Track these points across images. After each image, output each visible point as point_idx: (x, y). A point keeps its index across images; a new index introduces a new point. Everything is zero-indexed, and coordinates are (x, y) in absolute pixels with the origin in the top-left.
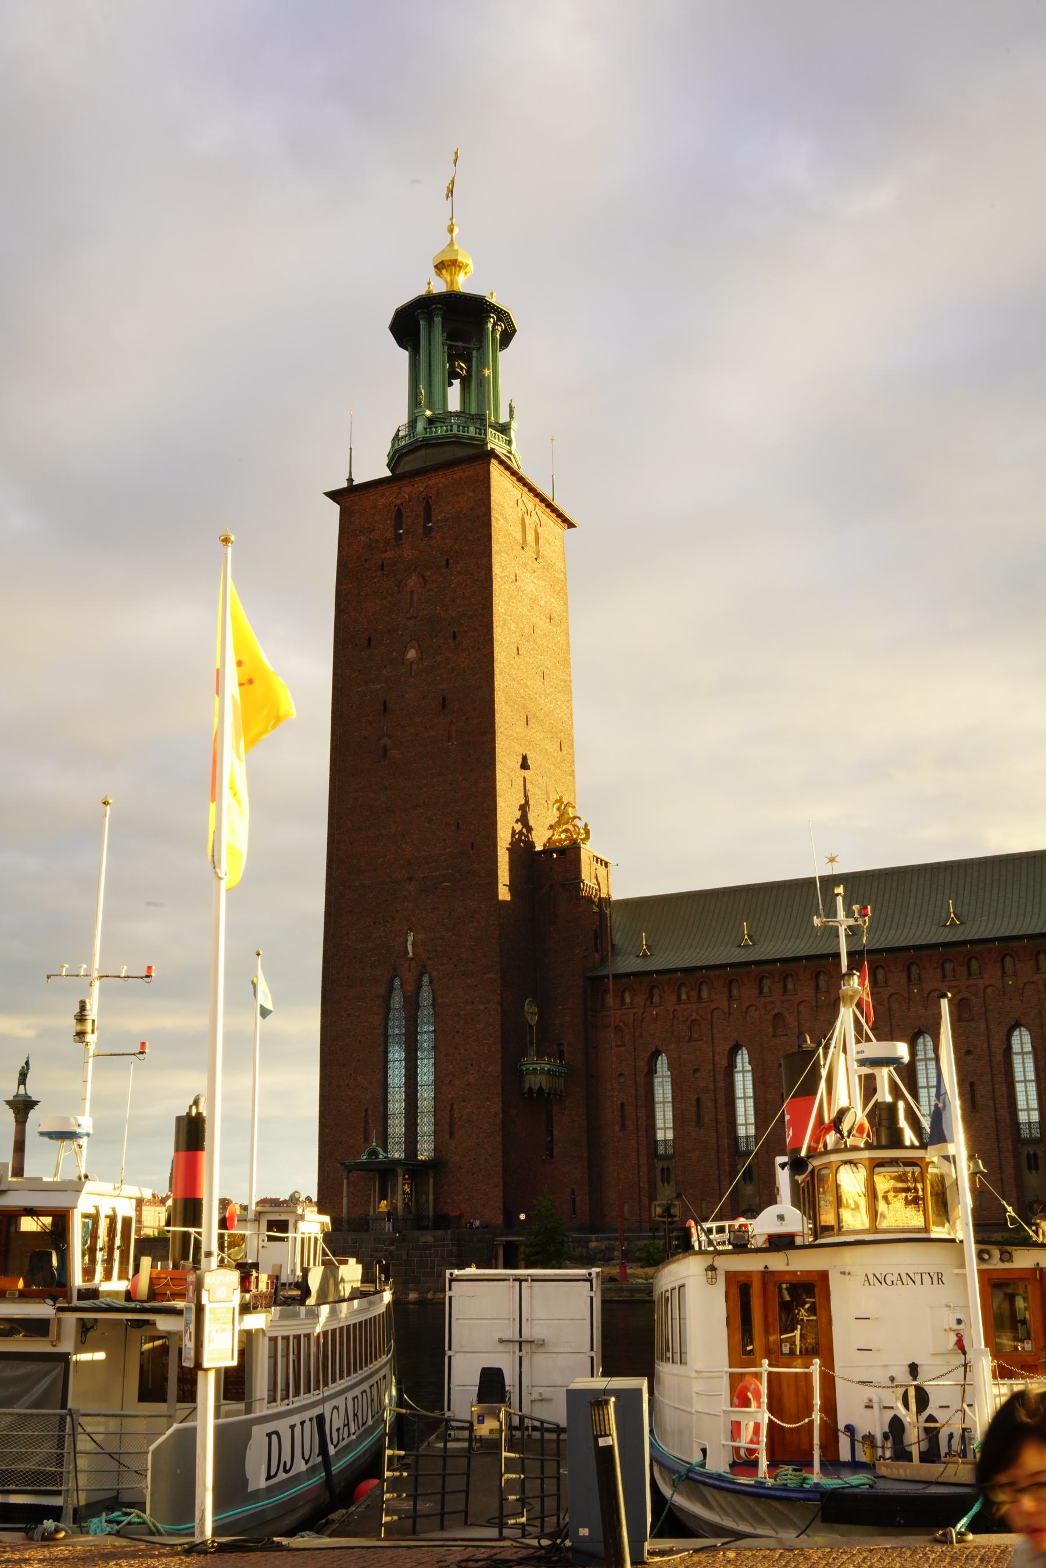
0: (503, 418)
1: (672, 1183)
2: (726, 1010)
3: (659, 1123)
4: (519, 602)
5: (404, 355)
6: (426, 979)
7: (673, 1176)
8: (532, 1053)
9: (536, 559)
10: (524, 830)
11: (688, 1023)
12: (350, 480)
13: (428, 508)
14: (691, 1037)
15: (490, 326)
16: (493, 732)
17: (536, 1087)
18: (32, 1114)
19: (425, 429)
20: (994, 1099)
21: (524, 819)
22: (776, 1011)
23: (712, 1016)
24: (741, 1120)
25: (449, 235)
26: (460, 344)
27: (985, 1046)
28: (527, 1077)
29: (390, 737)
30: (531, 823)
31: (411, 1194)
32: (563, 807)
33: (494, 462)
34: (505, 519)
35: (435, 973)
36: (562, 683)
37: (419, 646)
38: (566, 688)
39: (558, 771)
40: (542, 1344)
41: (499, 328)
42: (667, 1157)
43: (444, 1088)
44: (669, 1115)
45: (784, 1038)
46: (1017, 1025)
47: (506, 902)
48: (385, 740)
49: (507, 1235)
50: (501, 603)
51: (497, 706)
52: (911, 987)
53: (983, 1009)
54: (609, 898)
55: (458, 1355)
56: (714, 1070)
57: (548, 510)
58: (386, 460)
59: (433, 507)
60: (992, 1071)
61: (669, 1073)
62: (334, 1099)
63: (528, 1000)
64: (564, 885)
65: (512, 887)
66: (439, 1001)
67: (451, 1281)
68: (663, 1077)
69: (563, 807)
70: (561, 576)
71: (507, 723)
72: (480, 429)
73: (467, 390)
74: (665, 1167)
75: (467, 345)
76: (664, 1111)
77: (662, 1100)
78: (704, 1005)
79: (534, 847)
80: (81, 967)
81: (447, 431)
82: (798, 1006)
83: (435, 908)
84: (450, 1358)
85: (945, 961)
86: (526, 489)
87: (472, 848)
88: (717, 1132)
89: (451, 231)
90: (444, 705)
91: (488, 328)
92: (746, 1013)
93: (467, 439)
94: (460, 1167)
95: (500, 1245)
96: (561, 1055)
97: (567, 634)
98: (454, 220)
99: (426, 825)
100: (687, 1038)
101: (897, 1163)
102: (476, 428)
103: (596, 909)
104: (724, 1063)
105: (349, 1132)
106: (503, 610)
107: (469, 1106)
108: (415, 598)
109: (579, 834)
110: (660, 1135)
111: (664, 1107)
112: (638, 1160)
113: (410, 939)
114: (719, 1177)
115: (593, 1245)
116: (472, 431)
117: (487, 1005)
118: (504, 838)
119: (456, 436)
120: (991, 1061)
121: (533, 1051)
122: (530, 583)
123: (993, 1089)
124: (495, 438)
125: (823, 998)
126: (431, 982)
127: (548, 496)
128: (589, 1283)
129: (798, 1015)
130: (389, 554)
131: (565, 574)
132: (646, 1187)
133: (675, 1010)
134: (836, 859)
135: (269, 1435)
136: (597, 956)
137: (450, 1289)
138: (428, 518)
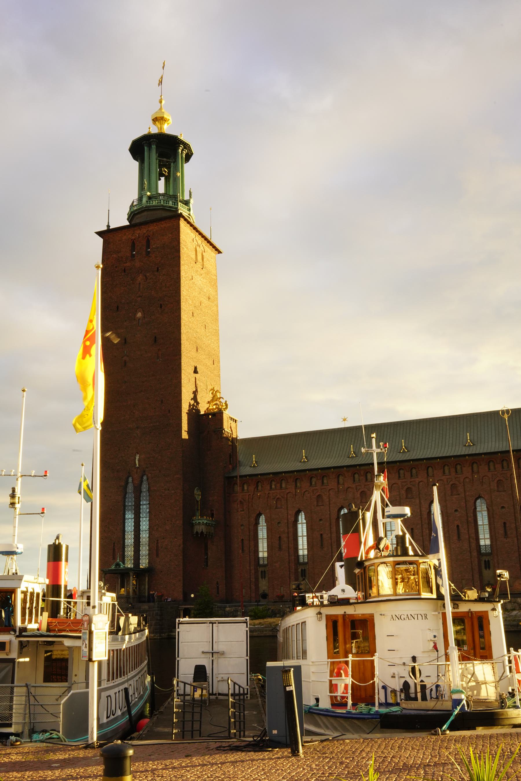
0: (186, 198)
1: (267, 578)
2: (294, 493)
3: (260, 549)
4: (194, 290)
5: (136, 164)
6: (145, 478)
7: (267, 575)
9: (202, 268)
10: (195, 404)
11: (275, 500)
12: (108, 226)
13: (148, 242)
15: (180, 151)
16: (180, 355)
17: (200, 531)
19: (147, 202)
20: (423, 536)
21: (195, 398)
22: (318, 494)
23: (287, 496)
24: (300, 547)
25: (160, 104)
26: (165, 159)
27: (419, 511)
30: (199, 400)
31: (137, 585)
32: (214, 392)
33: (182, 219)
34: (187, 248)
35: (150, 475)
36: (215, 331)
38: (216, 333)
39: (212, 375)
40: (223, 653)
41: (185, 152)
42: (264, 566)
43: (154, 532)
44: (265, 545)
45: (321, 507)
46: (479, 497)
47: (185, 439)
49: (185, 605)
50: (185, 290)
51: (182, 342)
54: (237, 438)
55: (182, 660)
56: (288, 523)
57: (208, 244)
58: (127, 217)
59: (151, 241)
61: (266, 524)
63: (196, 489)
64: (215, 431)
65: (189, 432)
66: (152, 489)
67: (179, 624)
68: (262, 526)
69: (215, 393)
70: (214, 277)
71: (187, 350)
72: (175, 203)
73: (168, 183)
74: (263, 570)
75: (168, 160)
76: (263, 543)
77: (262, 537)
78: (283, 490)
79: (200, 412)
80: (12, 471)
81: (158, 203)
82: (329, 491)
84: (178, 661)
85: (400, 469)
86: (197, 234)
87: (169, 412)
88: (289, 554)
89: (161, 102)
90: (155, 341)
91: (179, 152)
93: (167, 207)
94: (161, 572)
95: (181, 610)
96: (212, 515)
97: (217, 306)
98: (162, 97)
100: (275, 507)
101: (406, 563)
102: (173, 202)
103: (230, 443)
104: (293, 519)
106: (186, 294)
108: (141, 287)
109: (222, 406)
110: (261, 555)
111: (263, 541)
112: (250, 567)
113: (137, 457)
115: (228, 609)
116: (171, 204)
118: (185, 408)
119: (162, 206)
120: (421, 518)
121: (198, 513)
122: (199, 281)
123: (422, 532)
124: (182, 207)
126: (148, 479)
127: (208, 237)
128: (246, 624)
130: (128, 264)
131: (216, 276)
132: (254, 580)
133: (269, 493)
134: (347, 419)
135: (107, 697)
136: (230, 466)
137: (178, 628)
138: (148, 246)
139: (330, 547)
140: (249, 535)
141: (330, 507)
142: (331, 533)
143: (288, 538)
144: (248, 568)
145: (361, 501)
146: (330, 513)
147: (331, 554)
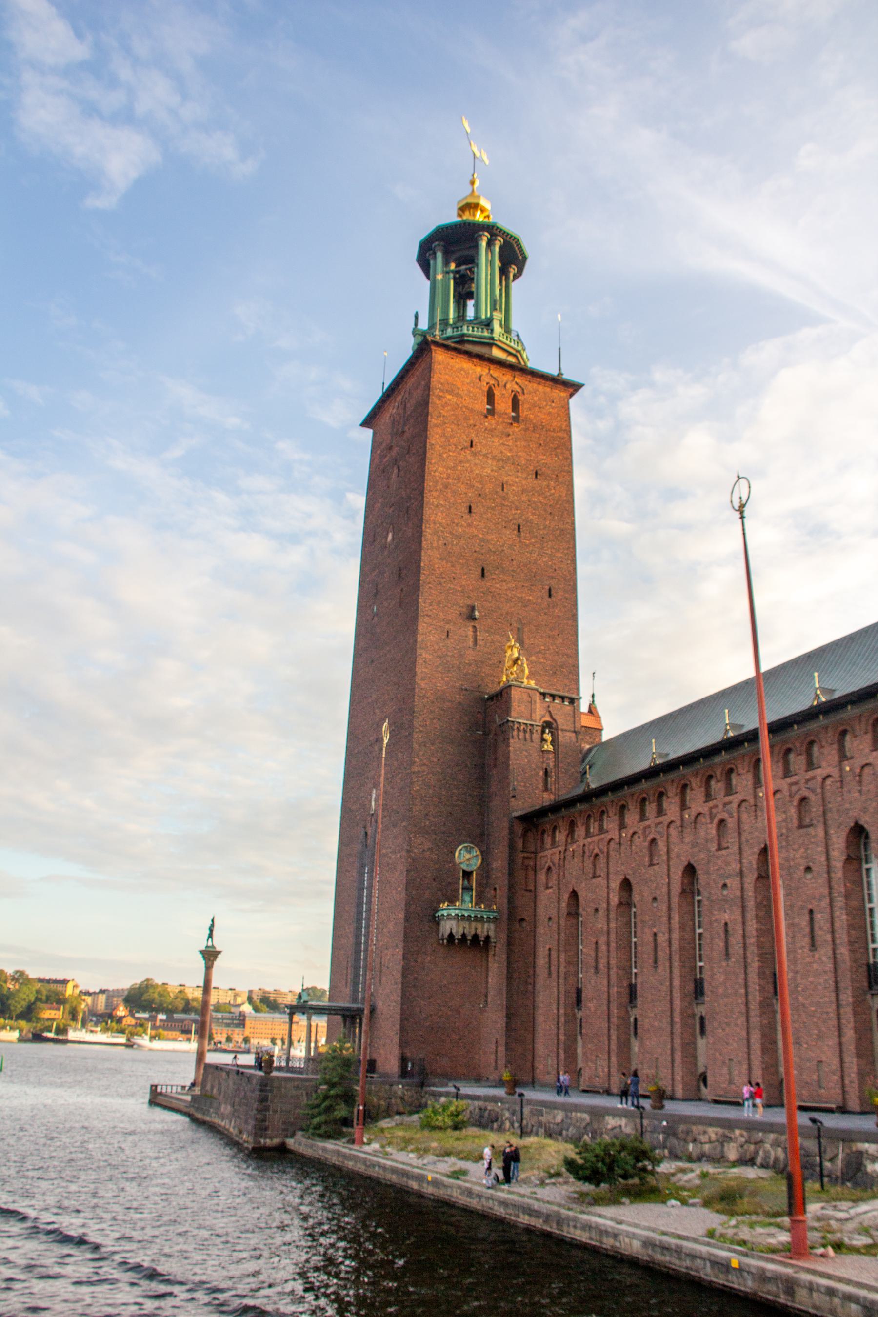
8: (467, 898)
11: (592, 858)
14: (594, 873)
18: (218, 963)
20: (833, 932)
22: (651, 836)
27: (823, 859)
28: (442, 923)
34: (457, 395)
50: (440, 469)
52: (758, 790)
53: (821, 809)
60: (830, 893)
71: (443, 578)
78: (603, 836)
82: (668, 826)
92: (631, 841)
100: (591, 875)
112: (558, 1009)
114: (609, 1030)
129: (668, 838)
133: (584, 845)
139: (667, 964)
140: (558, 940)
141: (668, 866)
142: (670, 930)
143: (608, 944)
144: (555, 1011)
145: (719, 845)
146: (669, 884)
147: (668, 984)
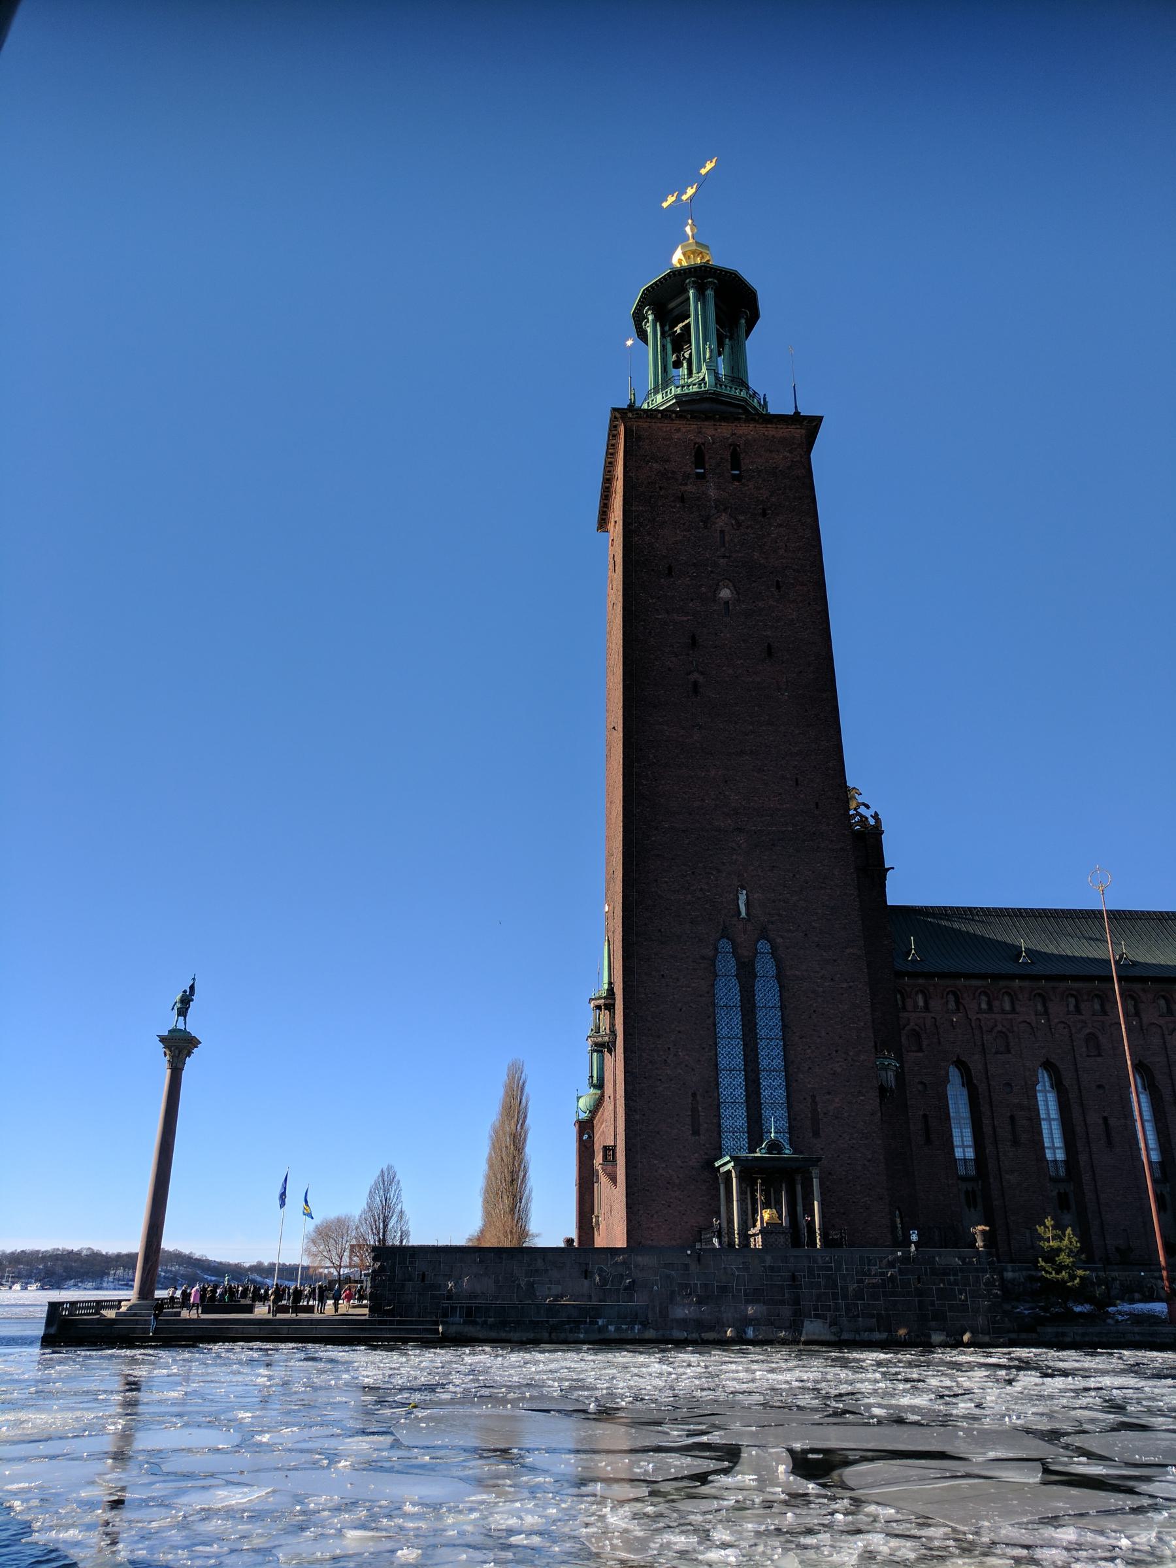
22: (1088, 1031)
29: (702, 673)
37: (735, 587)
48: (696, 675)
62: (645, 1078)
83: (773, 867)
87: (817, 808)
94: (830, 1174)
99: (756, 774)
105: (669, 1120)
107: (837, 1100)
108: (727, 538)
113: (742, 898)
117: (852, 984)
125: (1134, 1023)
130: (689, 488)
